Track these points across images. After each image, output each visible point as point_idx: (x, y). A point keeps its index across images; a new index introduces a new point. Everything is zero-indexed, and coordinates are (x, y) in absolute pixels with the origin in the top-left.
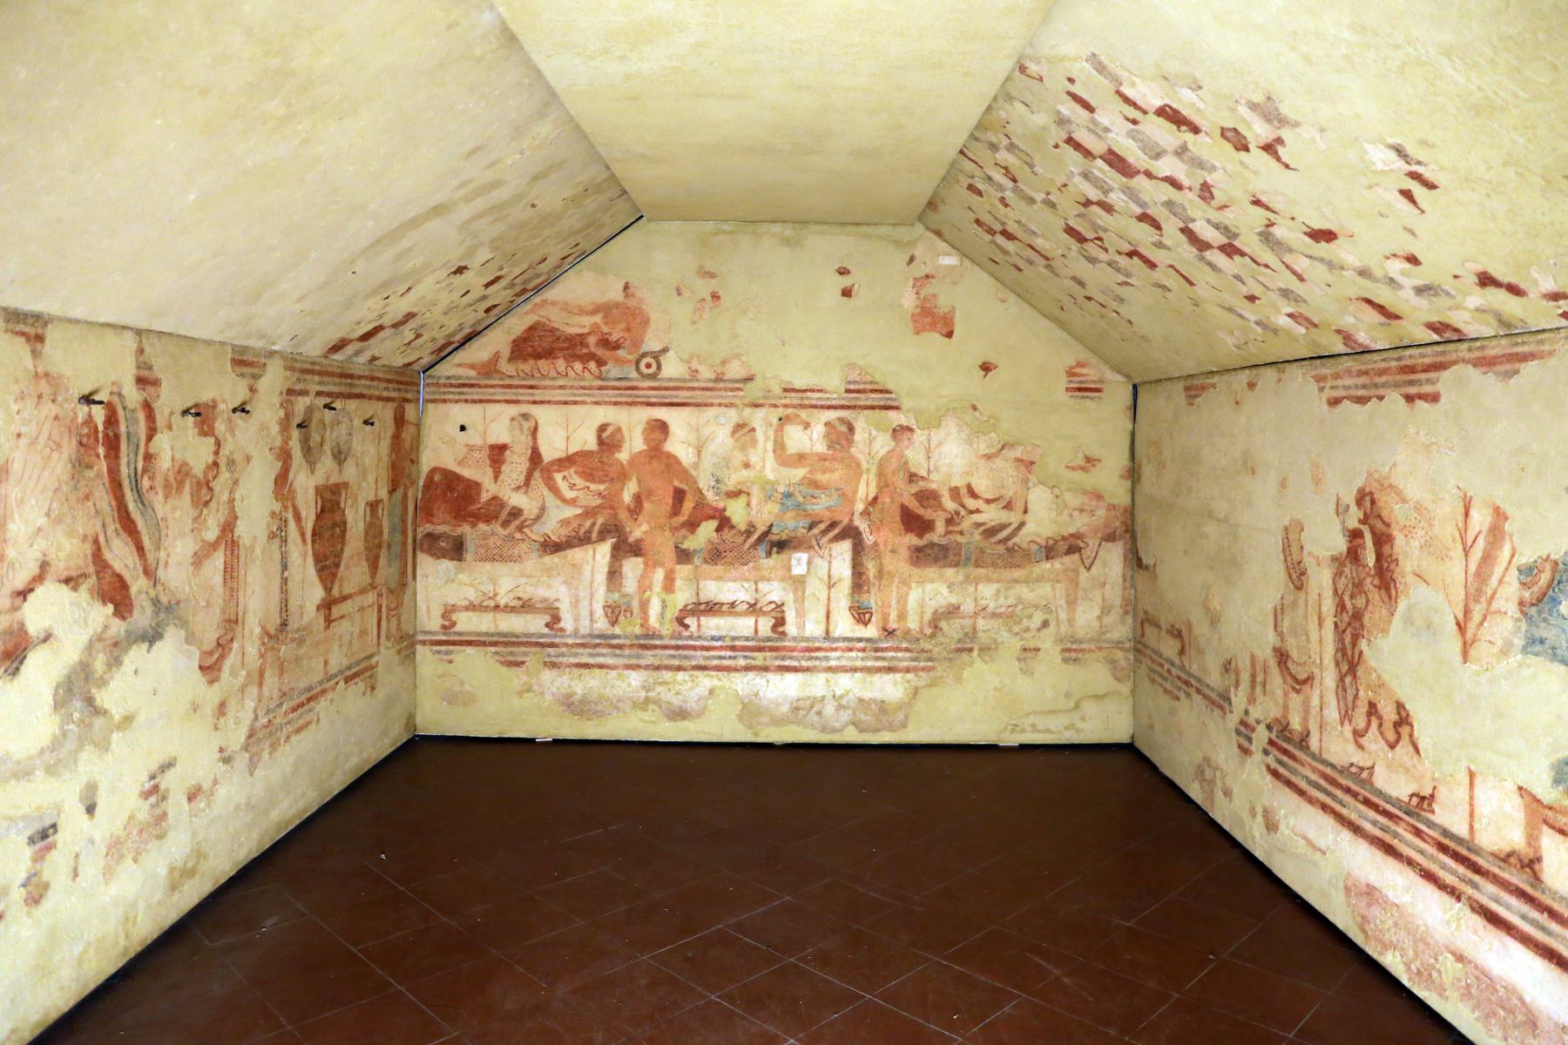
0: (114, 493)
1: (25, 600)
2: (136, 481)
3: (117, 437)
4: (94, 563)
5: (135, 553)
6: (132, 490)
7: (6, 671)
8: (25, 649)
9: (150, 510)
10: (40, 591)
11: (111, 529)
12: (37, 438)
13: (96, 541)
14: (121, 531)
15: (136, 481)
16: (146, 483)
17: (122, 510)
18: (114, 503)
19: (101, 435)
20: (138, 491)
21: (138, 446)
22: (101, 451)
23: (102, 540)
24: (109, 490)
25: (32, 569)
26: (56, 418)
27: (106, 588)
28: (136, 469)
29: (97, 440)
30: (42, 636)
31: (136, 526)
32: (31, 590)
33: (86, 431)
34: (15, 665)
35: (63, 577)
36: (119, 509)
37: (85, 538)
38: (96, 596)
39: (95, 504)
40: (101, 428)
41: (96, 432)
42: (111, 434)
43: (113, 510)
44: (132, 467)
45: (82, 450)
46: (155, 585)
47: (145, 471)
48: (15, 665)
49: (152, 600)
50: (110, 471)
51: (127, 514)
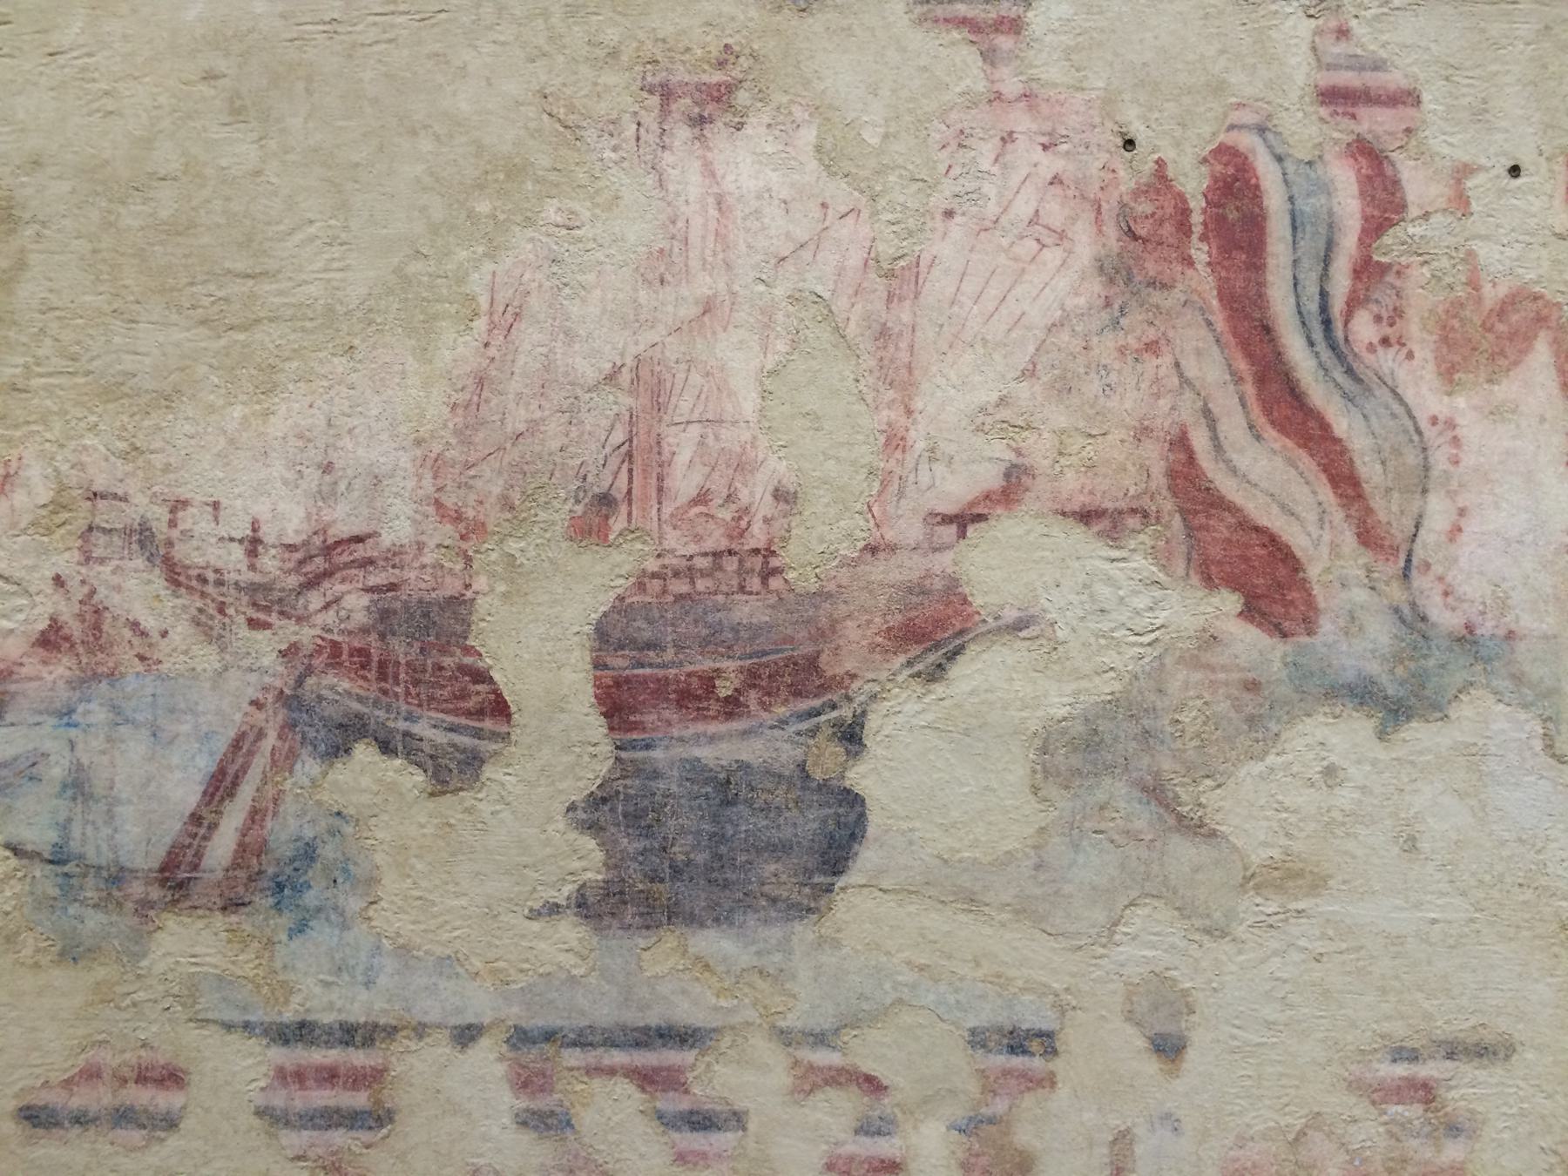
0: (1245, 346)
1: (962, 534)
2: (1327, 323)
3: (1255, 223)
4: (1174, 490)
5: (1326, 494)
6: (1311, 344)
7: (909, 664)
8: (961, 632)
9: (1383, 394)
10: (1007, 528)
11: (1233, 426)
12: (996, 222)
13: (1181, 442)
14: (1270, 433)
15: (1327, 323)
16: (1364, 329)
17: (1274, 387)
18: (1242, 365)
19: (1197, 219)
20: (1333, 347)
21: (1330, 245)
22: (1200, 253)
23: (1200, 440)
24: (1229, 338)
25: (990, 477)
26: (1056, 180)
27: (1216, 552)
28: (1324, 294)
29: (1184, 227)
30: (1010, 615)
31: (1325, 427)
32: (980, 518)
33: (1144, 207)
34: (932, 658)
35: (1075, 506)
36: (1261, 381)
37: (1143, 432)
38: (1180, 567)
39: (1177, 365)
40: (1197, 204)
41: (1185, 212)
42: (1233, 216)
43: (1239, 380)
44: (1311, 289)
45: (1132, 246)
46: (1406, 575)
47: (1353, 304)
48: (932, 658)
49: (1397, 610)
50: (1228, 298)
51: (1295, 396)
